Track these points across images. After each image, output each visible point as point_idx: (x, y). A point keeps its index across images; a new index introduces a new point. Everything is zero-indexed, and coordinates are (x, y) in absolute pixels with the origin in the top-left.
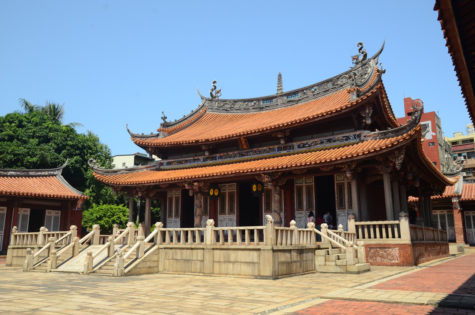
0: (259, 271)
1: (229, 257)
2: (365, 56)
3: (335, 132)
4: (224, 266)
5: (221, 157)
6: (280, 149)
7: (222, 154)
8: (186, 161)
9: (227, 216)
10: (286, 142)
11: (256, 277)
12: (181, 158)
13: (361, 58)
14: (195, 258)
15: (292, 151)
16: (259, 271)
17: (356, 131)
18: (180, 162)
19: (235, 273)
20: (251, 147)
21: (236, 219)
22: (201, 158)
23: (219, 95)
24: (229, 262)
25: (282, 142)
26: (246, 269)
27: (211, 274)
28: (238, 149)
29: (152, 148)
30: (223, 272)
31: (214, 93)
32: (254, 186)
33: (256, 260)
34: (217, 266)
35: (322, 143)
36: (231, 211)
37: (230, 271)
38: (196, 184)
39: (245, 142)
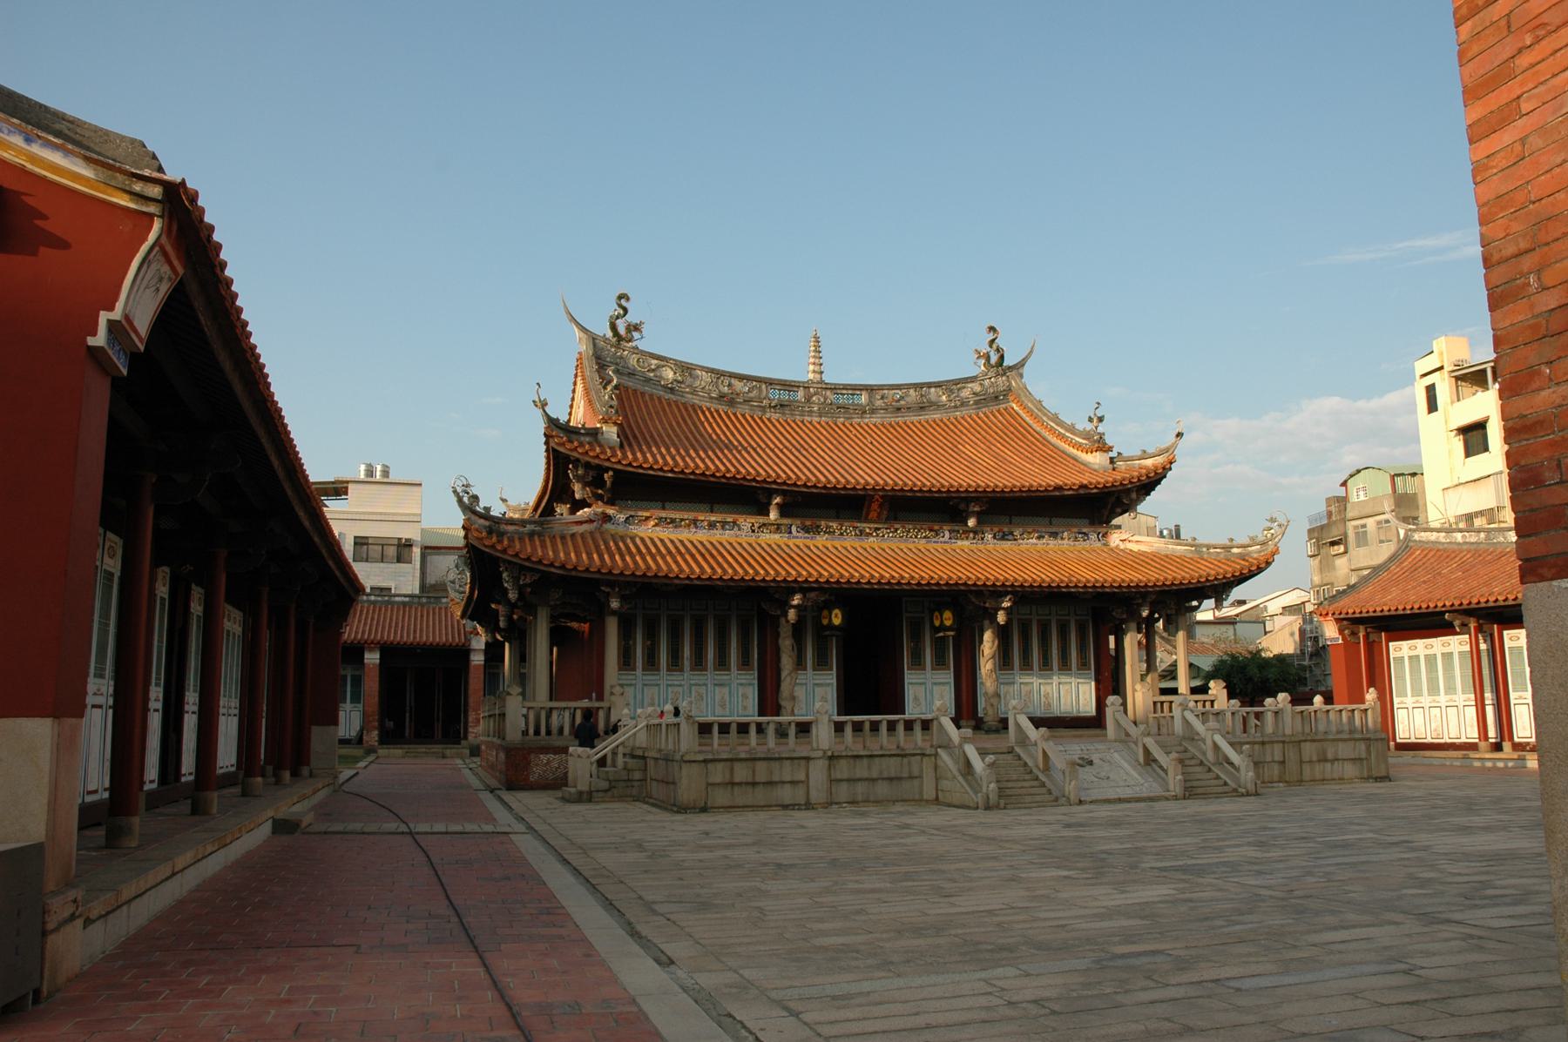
0: (1370, 769)
1: (1325, 752)
2: (1002, 357)
3: (1055, 521)
4: (1318, 768)
5: (806, 530)
6: (955, 534)
7: (808, 523)
8: (695, 522)
9: (809, 676)
10: (979, 522)
11: (1367, 779)
12: (664, 508)
13: (994, 358)
14: (1269, 759)
15: (981, 547)
16: (1370, 769)
17: (1092, 523)
18: (673, 521)
19: (1336, 776)
20: (887, 520)
21: (834, 681)
22: (746, 522)
23: (636, 335)
24: (1326, 760)
25: (971, 522)
26: (1350, 770)
27: (1301, 782)
28: (859, 520)
29: (587, 466)
30: (1318, 776)
31: (622, 330)
32: (948, 615)
33: (1364, 755)
34: (1307, 769)
35: (1039, 538)
36: (821, 663)
37: (1328, 776)
38: (812, 595)
39: (880, 506)
